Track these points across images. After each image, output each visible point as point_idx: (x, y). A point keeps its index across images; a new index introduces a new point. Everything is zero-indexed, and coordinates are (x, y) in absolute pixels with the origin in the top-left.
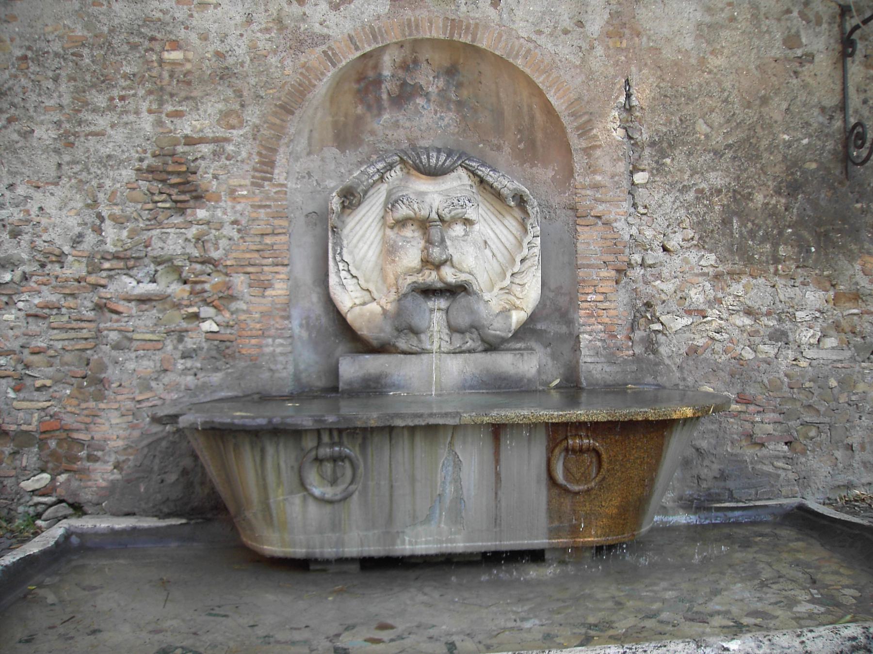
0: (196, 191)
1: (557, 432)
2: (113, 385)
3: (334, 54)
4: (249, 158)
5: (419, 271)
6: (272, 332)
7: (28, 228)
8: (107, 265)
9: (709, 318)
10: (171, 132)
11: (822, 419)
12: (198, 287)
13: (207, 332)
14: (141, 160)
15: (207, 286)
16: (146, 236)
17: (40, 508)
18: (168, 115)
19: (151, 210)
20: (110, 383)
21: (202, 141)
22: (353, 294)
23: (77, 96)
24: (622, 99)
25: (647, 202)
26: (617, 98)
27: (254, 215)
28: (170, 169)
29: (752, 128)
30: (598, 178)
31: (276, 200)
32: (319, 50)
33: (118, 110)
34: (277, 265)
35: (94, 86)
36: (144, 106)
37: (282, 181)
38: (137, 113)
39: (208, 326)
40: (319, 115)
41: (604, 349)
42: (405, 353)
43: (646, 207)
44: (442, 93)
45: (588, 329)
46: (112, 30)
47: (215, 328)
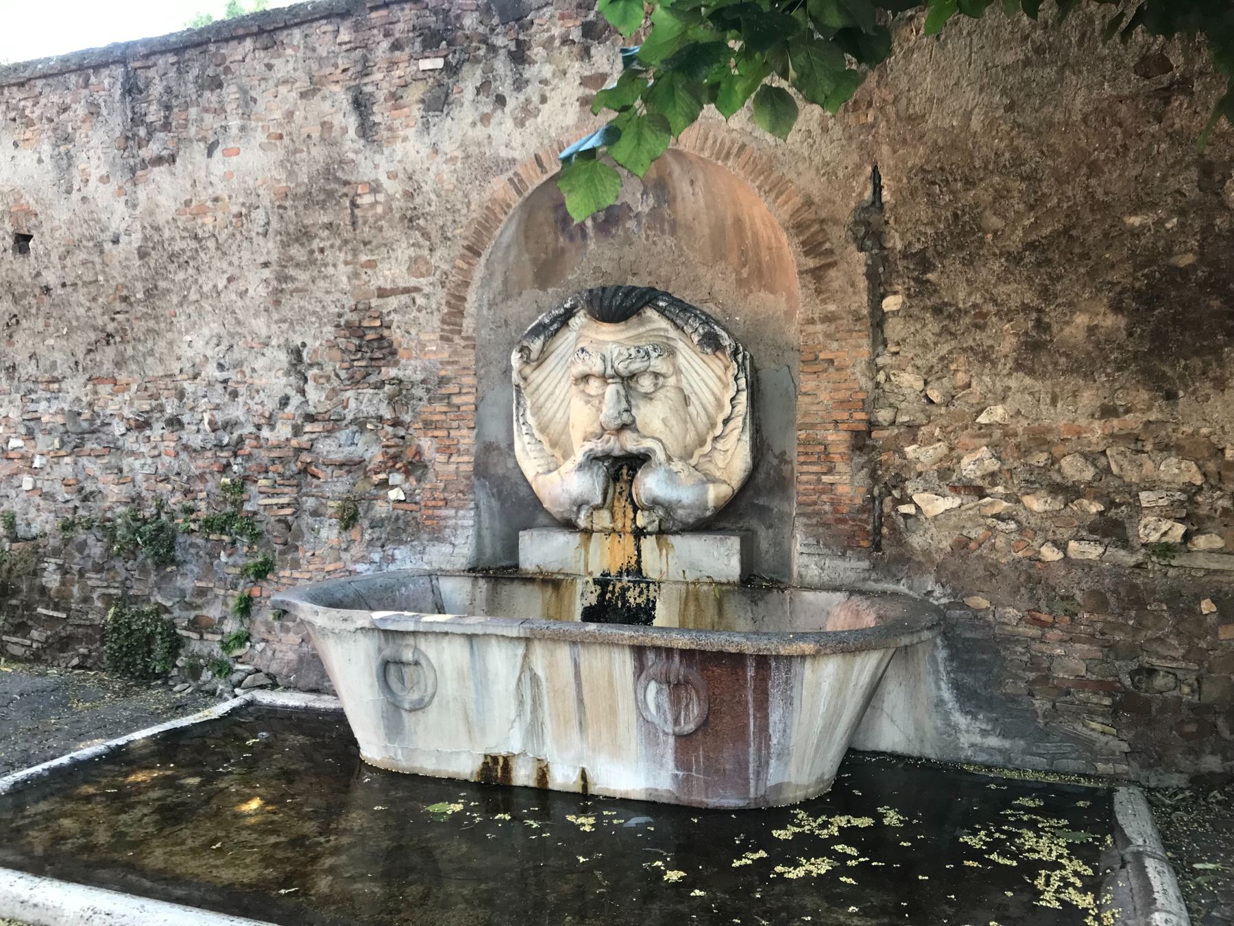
3: (521, 181)
14: (340, 315)
21: (394, 292)
28: (365, 323)
35: (297, 240)
39: (394, 494)
43: (898, 344)
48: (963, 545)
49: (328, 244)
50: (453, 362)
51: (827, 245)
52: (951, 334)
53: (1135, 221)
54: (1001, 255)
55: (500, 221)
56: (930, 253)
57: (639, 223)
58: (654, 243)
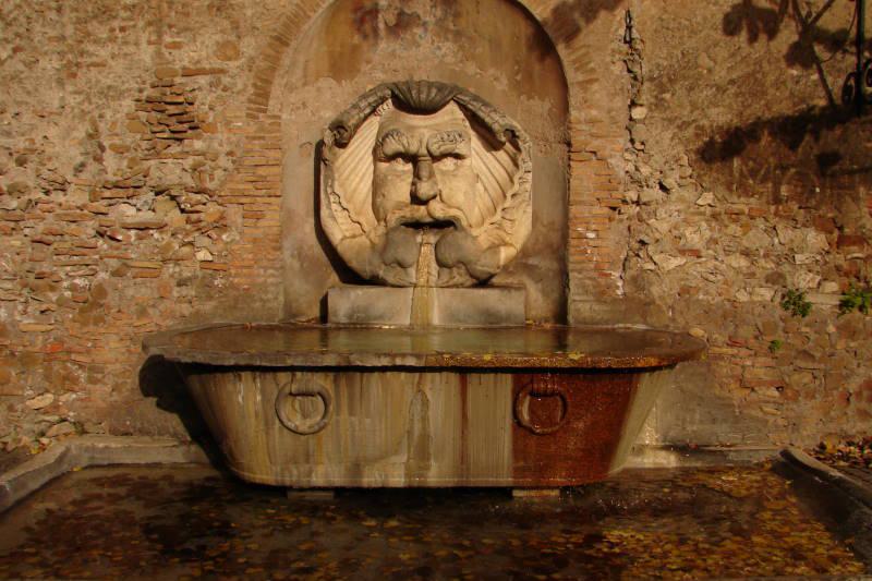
1: (524, 377)
6: (265, 263)
7: (34, 157)
8: (107, 194)
9: (704, 259)
10: (169, 63)
11: (816, 366)
12: (194, 217)
15: (202, 216)
16: (146, 164)
17: (43, 426)
18: (166, 46)
20: (109, 308)
22: (344, 227)
24: (622, 32)
25: (643, 138)
26: (617, 30)
27: (250, 146)
29: (758, 62)
30: (594, 112)
31: (270, 132)
33: (119, 40)
34: (270, 196)
35: (95, 17)
36: (144, 38)
37: (276, 113)
38: (137, 44)
39: (202, 255)
40: (315, 45)
41: (594, 287)
42: (393, 286)
43: (643, 143)
44: (440, 22)
45: (578, 267)
47: (210, 258)
48: (685, 291)
49: (132, 23)
50: (260, 138)
51: (592, 65)
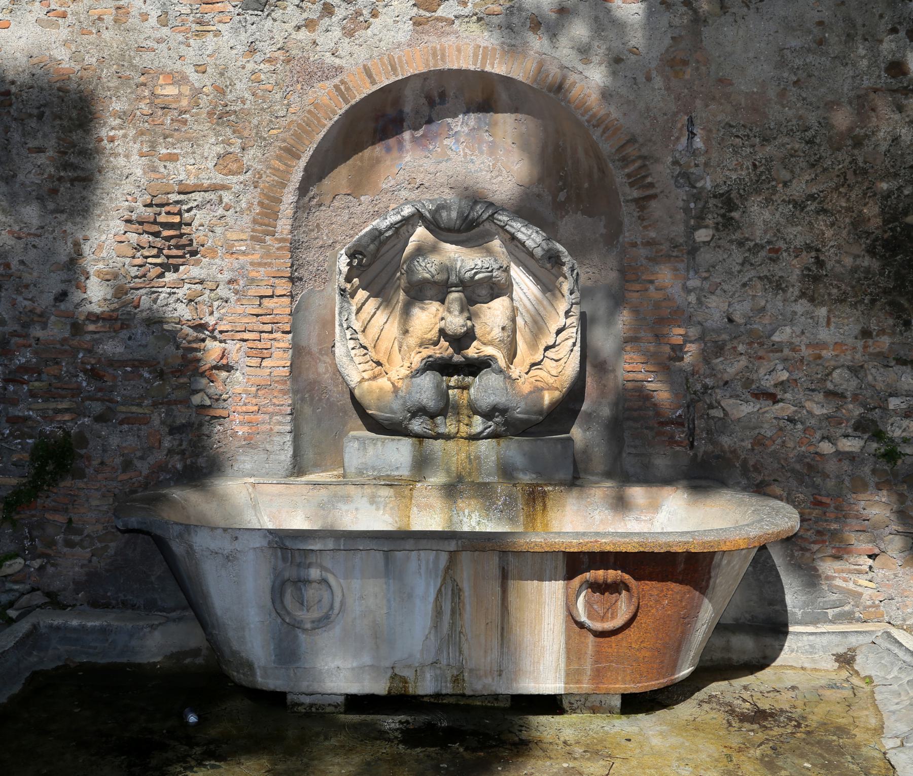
0: (191, 245)
2: (94, 463)
3: (348, 89)
4: (249, 209)
5: (436, 343)
6: (271, 409)
13: (198, 406)
19: (140, 266)
23: (63, 136)
28: (162, 218)
32: (329, 84)
46: (101, 60)
49: (121, 132)
51: (649, 180)
52: (752, 264)
53: (884, 186)
54: (789, 202)
55: (324, 125)
56: (734, 195)
57: (457, 141)
58: (472, 161)
